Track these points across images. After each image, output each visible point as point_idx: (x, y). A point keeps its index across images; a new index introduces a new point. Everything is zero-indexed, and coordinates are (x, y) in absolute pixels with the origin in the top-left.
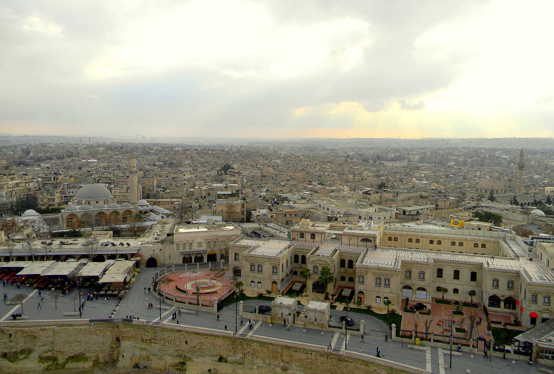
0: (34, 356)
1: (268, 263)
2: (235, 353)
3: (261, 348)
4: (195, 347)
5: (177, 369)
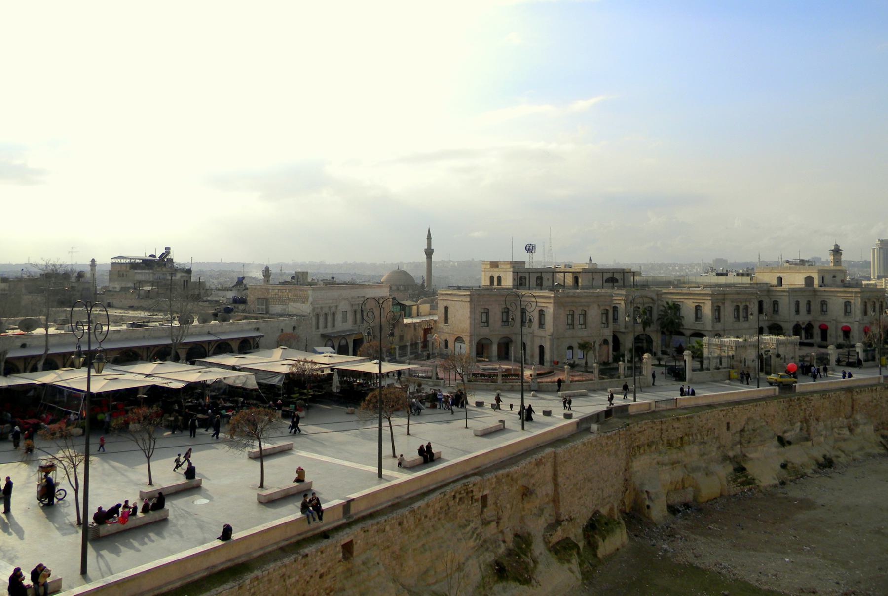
0: (538, 548)
1: (596, 306)
2: (792, 424)
3: (822, 400)
4: (743, 430)
5: (743, 484)
